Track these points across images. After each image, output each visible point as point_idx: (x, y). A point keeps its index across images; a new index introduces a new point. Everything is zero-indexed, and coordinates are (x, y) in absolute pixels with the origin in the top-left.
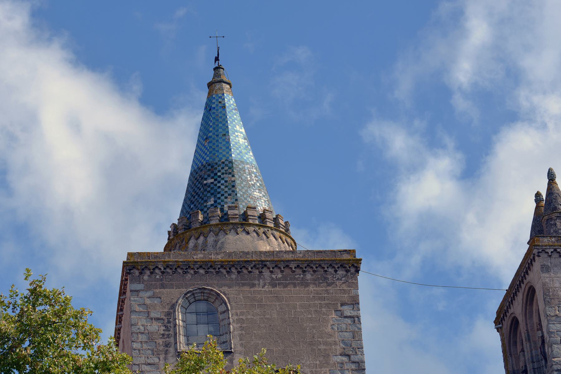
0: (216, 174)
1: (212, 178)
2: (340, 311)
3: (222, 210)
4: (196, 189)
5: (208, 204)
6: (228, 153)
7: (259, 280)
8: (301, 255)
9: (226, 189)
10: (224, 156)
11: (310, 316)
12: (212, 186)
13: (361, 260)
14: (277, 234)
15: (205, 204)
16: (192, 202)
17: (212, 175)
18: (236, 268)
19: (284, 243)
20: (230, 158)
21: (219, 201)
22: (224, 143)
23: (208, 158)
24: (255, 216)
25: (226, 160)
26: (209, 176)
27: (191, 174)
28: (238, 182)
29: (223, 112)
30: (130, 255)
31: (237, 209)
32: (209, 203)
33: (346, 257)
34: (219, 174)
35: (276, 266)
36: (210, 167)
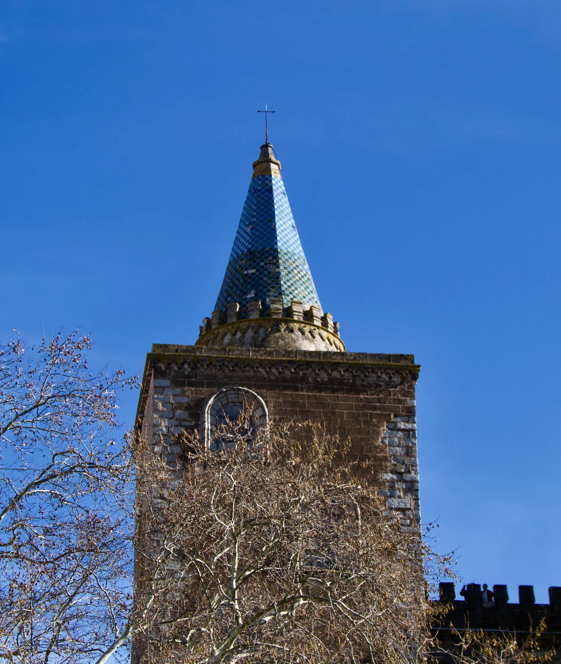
0: (258, 264)
1: (254, 268)
2: (393, 422)
3: (263, 304)
4: (235, 280)
5: (247, 297)
6: (273, 241)
7: (302, 384)
8: (352, 358)
9: (270, 282)
10: (269, 244)
11: (358, 427)
12: (253, 277)
13: (419, 366)
14: (324, 334)
15: (244, 297)
16: (229, 295)
17: (254, 265)
18: (277, 369)
19: (331, 344)
20: (275, 247)
21: (260, 294)
22: (269, 230)
23: (250, 246)
24: (300, 312)
25: (271, 249)
26: (250, 265)
27: (230, 263)
28: (283, 274)
29: (270, 196)
30: (156, 346)
31: (281, 303)
32: (249, 296)
33: (403, 363)
34: (262, 264)
35: (322, 368)
36: (251, 256)
